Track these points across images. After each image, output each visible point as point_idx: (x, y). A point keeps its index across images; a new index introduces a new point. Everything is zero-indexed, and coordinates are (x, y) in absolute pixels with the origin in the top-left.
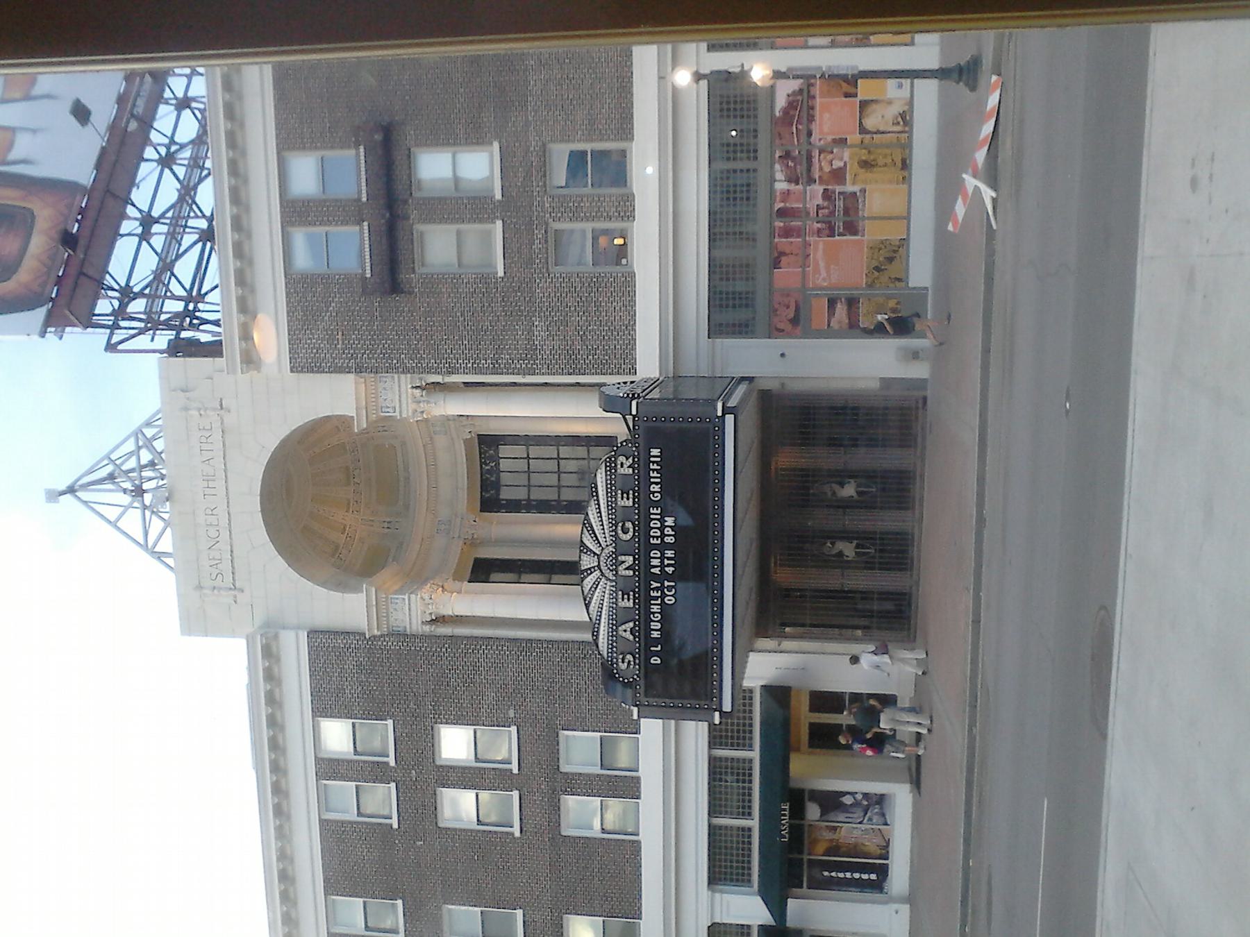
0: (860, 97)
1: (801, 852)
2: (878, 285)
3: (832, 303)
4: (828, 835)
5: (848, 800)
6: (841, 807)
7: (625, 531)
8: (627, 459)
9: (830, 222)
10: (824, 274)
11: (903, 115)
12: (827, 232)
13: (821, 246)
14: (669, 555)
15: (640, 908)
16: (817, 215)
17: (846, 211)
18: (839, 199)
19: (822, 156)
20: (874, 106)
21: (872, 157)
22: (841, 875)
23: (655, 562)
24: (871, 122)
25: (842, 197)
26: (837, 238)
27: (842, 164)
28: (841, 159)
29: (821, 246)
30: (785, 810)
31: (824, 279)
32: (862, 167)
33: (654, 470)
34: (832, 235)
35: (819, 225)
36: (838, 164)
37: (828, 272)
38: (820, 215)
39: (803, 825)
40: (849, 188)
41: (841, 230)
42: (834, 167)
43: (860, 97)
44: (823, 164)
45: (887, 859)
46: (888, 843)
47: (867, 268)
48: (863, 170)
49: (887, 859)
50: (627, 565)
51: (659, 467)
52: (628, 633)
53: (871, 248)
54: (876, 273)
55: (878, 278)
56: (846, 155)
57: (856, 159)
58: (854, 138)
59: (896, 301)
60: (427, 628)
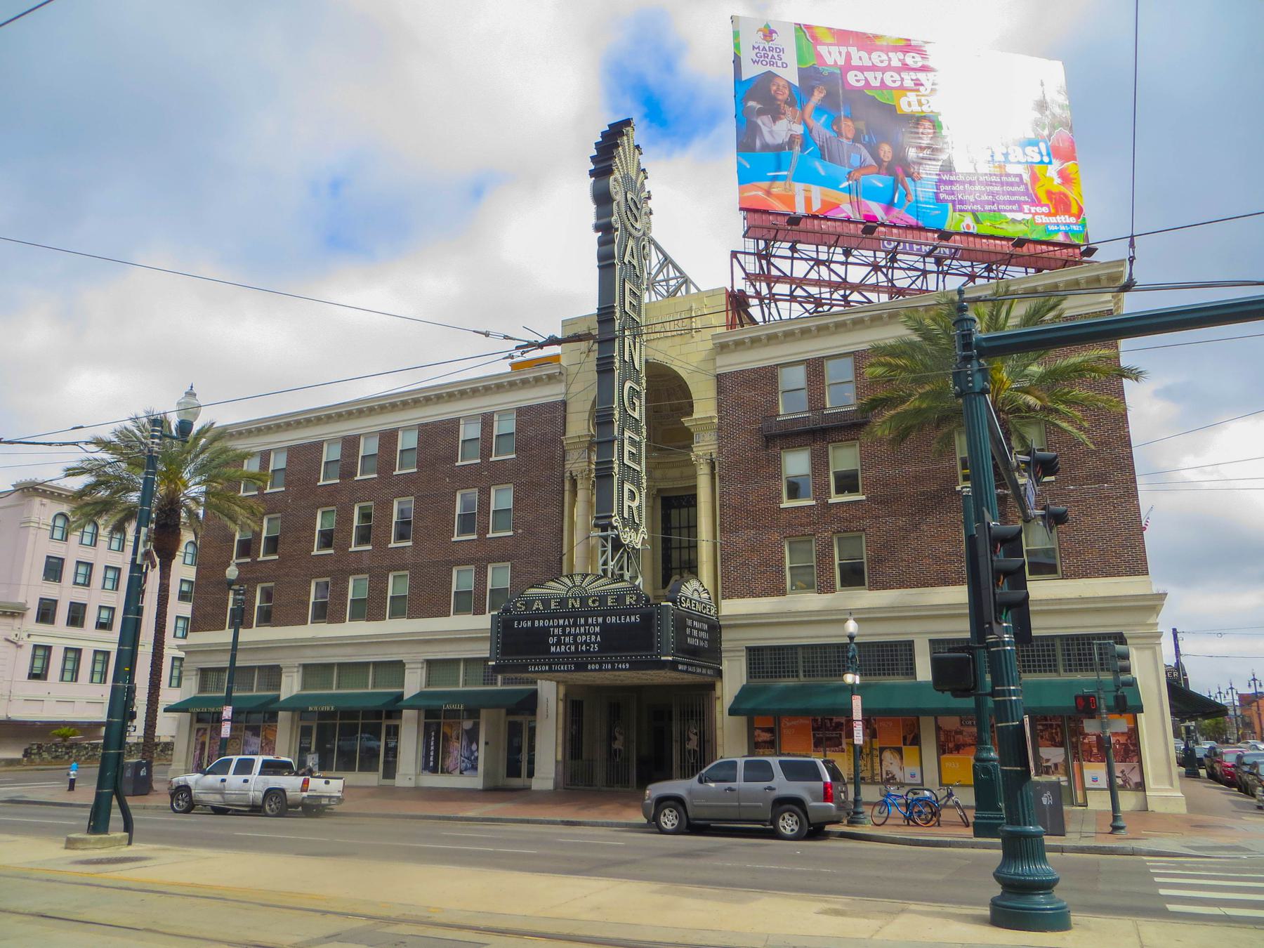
0: (904, 748)
3: (770, 730)
4: (454, 734)
5: (474, 747)
6: (470, 742)
7: (594, 602)
10: (788, 724)
11: (893, 778)
12: (815, 726)
17: (829, 739)
20: (898, 757)
21: (864, 756)
22: (432, 744)
23: (561, 622)
24: (887, 755)
29: (808, 722)
31: (785, 724)
35: (820, 720)
43: (904, 748)
45: (442, 772)
46: (449, 773)
49: (442, 772)
58: (877, 744)
60: (568, 474)
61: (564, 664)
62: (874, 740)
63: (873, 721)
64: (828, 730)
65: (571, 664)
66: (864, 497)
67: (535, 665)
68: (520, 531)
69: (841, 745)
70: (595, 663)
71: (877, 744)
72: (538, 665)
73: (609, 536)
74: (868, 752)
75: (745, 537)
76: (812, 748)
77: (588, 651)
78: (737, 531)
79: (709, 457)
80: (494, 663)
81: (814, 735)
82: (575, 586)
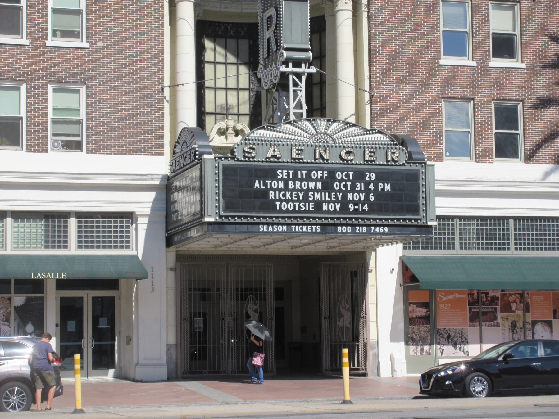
0: (554, 321)
2: (439, 338)
3: (426, 305)
8: (397, 157)
9: (478, 302)
12: (472, 300)
13: (464, 296)
14: (292, 184)
16: (482, 293)
17: (485, 313)
18: (492, 308)
19: (518, 295)
20: (548, 330)
21: (518, 330)
25: (494, 310)
26: (468, 307)
27: (514, 309)
28: (517, 309)
29: (464, 296)
30: (60, 275)
31: (441, 299)
32: (512, 323)
33: (322, 173)
34: (470, 304)
35: (476, 295)
36: (514, 306)
37: (448, 301)
38: (482, 295)
40: (499, 315)
41: (473, 310)
42: (512, 304)
43: (554, 321)
44: (513, 296)
47: (450, 330)
48: (510, 325)
50: (323, 154)
51: (324, 178)
52: (273, 153)
53: (462, 332)
54: (446, 336)
55: (443, 337)
56: (520, 312)
57: (517, 319)
58: (529, 318)
59: (428, 351)
61: (307, 225)
62: (527, 314)
63: (526, 295)
64: (484, 304)
65: (316, 225)
66: (523, 66)
67: (268, 224)
68: (100, 44)
69: (496, 318)
70: (347, 225)
72: (273, 224)
73: (303, 73)
74: (522, 326)
75: (400, 92)
76: (468, 323)
77: (356, 211)
80: (212, 220)
81: (470, 309)
82: (324, 134)
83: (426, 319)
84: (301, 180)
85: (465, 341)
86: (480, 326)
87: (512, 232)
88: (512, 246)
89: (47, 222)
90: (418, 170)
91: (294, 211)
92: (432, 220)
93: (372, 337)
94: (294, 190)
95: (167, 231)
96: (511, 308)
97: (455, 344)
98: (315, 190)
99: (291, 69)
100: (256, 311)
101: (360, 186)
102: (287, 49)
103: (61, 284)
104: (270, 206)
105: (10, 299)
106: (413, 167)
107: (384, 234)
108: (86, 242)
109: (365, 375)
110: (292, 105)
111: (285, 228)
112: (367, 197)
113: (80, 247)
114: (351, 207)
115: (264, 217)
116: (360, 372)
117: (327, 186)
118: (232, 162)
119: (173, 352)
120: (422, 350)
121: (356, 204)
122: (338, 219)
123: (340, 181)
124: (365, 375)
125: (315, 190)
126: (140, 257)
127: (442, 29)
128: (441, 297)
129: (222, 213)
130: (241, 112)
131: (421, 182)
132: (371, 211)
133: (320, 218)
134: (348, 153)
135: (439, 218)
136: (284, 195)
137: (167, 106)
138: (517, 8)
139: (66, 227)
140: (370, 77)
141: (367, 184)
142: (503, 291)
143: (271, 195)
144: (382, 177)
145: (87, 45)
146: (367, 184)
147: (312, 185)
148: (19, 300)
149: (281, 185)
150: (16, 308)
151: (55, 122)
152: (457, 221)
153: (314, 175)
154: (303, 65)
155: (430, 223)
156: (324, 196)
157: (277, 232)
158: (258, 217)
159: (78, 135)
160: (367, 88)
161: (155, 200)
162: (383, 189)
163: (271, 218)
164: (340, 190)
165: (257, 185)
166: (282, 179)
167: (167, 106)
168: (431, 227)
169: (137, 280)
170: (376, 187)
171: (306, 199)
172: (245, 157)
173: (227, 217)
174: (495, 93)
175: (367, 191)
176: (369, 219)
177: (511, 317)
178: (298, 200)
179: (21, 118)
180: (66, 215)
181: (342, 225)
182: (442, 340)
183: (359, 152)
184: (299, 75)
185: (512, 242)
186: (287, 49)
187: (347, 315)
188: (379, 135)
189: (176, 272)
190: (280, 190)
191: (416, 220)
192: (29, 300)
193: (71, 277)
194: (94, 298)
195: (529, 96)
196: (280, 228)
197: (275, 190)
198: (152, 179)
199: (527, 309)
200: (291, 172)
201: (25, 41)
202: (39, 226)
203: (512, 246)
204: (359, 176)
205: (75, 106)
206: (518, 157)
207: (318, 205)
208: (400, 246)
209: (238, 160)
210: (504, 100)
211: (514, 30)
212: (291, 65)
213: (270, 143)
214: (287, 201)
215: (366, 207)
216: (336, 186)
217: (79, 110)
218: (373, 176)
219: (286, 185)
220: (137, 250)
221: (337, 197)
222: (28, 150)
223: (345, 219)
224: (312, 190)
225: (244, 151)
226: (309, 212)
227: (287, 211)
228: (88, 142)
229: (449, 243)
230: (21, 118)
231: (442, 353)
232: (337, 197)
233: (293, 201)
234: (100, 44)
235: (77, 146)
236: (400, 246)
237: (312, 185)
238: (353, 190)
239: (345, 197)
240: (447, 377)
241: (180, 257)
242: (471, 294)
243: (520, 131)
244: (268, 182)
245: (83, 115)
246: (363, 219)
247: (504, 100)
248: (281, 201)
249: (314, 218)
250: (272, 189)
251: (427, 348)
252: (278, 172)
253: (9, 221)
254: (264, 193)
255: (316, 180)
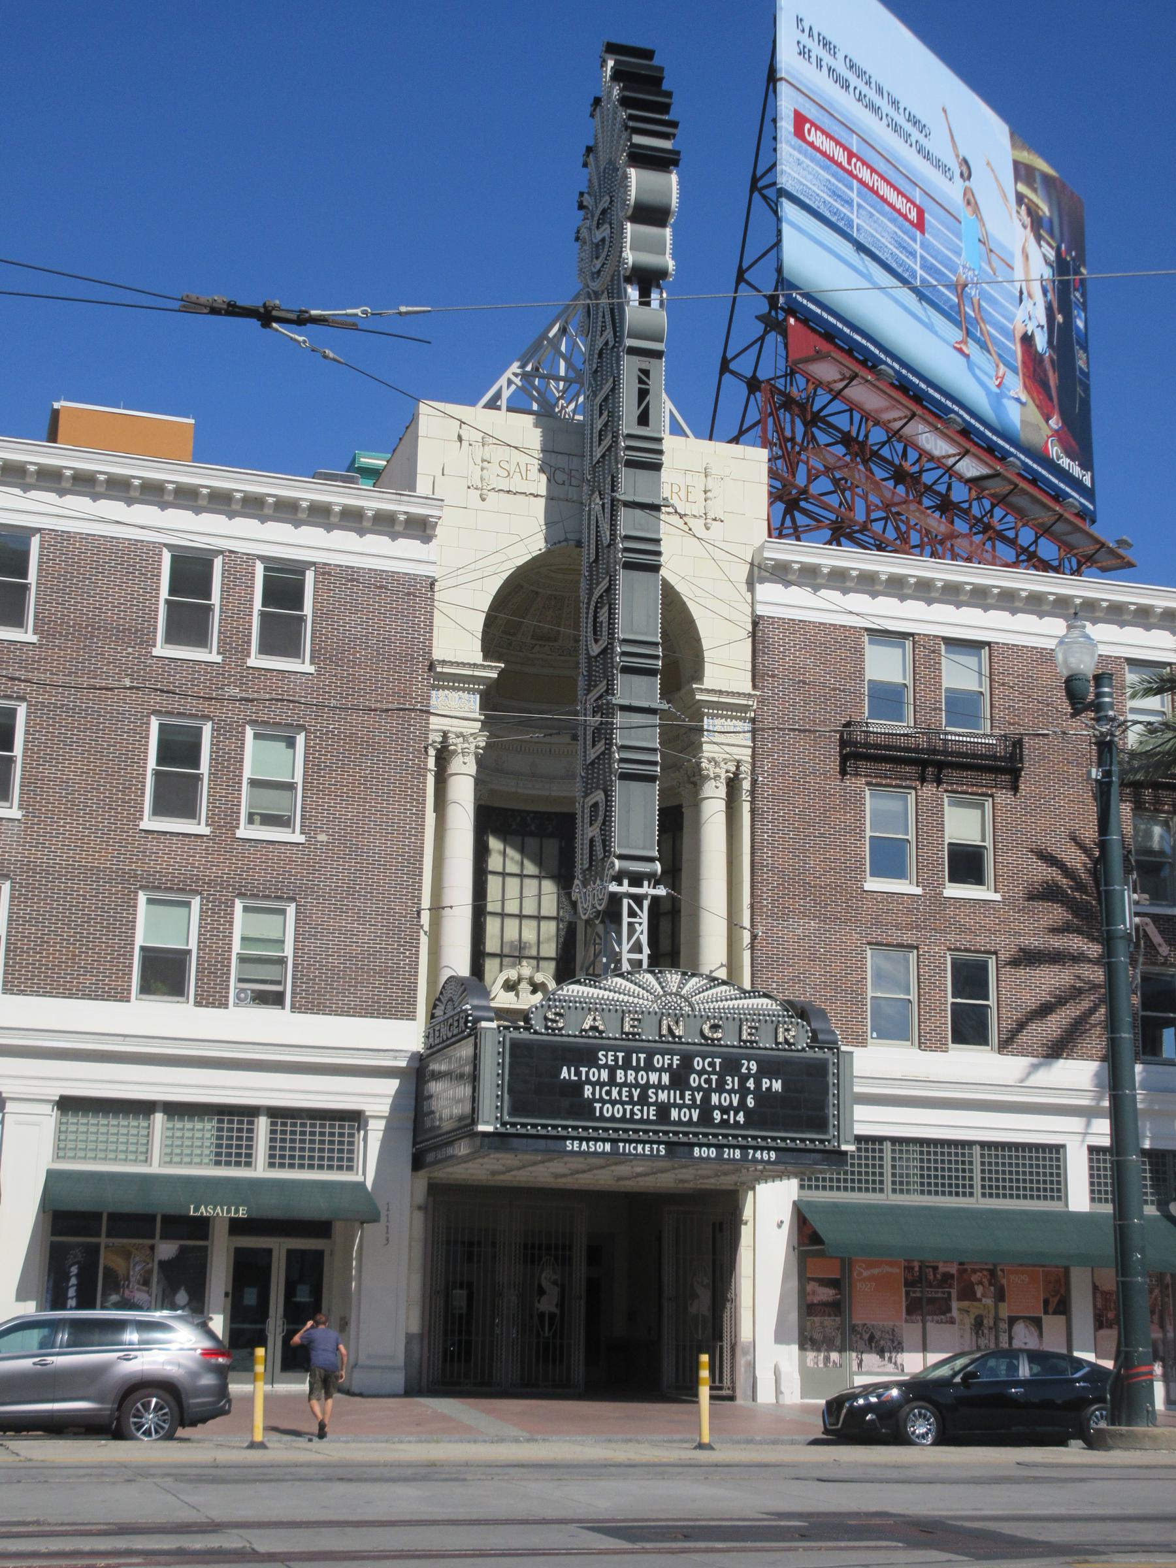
0: (1044, 1317)
1: (109, 1235)
2: (854, 1339)
3: (834, 1284)
4: (136, 1272)
7: (715, 1027)
8: (794, 1036)
9: (920, 1281)
10: (865, 1274)
13: (898, 1271)
15: (22, 992)
16: (928, 1267)
17: (931, 1301)
18: (943, 1293)
19: (986, 1273)
20: (1036, 1334)
25: (946, 1296)
26: (904, 1290)
27: (979, 1295)
28: (984, 1296)
29: (898, 1271)
30: (237, 1211)
31: (860, 1274)
32: (975, 1319)
33: (671, 1059)
34: (908, 1284)
35: (917, 1269)
36: (979, 1291)
38: (927, 1270)
39: (152, 1237)
40: (955, 1305)
41: (912, 1295)
42: (976, 1287)
43: (1044, 1317)
44: (979, 1274)
47: (873, 1326)
48: (973, 1322)
51: (675, 1067)
53: (893, 1330)
54: (866, 1337)
55: (861, 1338)
56: (989, 1301)
57: (984, 1313)
58: (1005, 1311)
59: (837, 1361)
61: (644, 1142)
62: (1001, 1305)
63: (1000, 1273)
64: (930, 1286)
65: (659, 1143)
66: (997, 897)
67: (581, 1139)
68: (322, 837)
69: (949, 1310)
70: (709, 1146)
71: (1004, 1313)
72: (588, 1140)
73: (645, 896)
74: (992, 1324)
75: (799, 931)
76: (904, 1315)
77: (724, 1123)
78: (784, 917)
79: (733, 769)
80: (490, 1129)
81: (907, 1293)
83: (835, 1308)
84: (637, 1069)
85: (899, 1348)
86: (924, 1322)
87: (977, 1167)
88: (978, 1190)
89: (220, 1121)
90: (827, 1060)
91: (623, 1119)
92: (847, 1142)
93: (745, 1334)
94: (625, 1084)
95: (415, 1143)
96: (974, 1293)
97: (881, 1352)
98: (659, 1086)
99: (625, 888)
100: (555, 1283)
101: (732, 1082)
102: (621, 857)
103: (237, 1227)
104: (584, 1110)
105: (152, 1248)
106: (819, 1054)
107: (769, 1162)
108: (282, 1157)
109: (732, 1398)
110: (626, 947)
111: (608, 1147)
112: (742, 1101)
113: (272, 1165)
114: (717, 1116)
115: (575, 1128)
116: (724, 1393)
117: (679, 1081)
118: (525, 1035)
119: (416, 1347)
120: (827, 1359)
121: (725, 1111)
122: (696, 1134)
123: (700, 1073)
124: (732, 1398)
125: (659, 1086)
126: (369, 1185)
127: (868, 833)
128: (861, 1272)
129: (506, 1118)
130: (543, 954)
131: (832, 1080)
132: (748, 1124)
133: (666, 1133)
134: (715, 1027)
135: (859, 1139)
136: (609, 1093)
137: (424, 941)
138: (988, 805)
139: (250, 1131)
140: (752, 907)
141: (744, 1079)
142: (961, 1264)
143: (588, 1091)
144: (768, 1068)
145: (301, 839)
146: (744, 1079)
147: (654, 1078)
148: (167, 1250)
149: (604, 1075)
150: (162, 1264)
151: (243, 959)
152: (887, 1146)
153: (658, 1061)
154: (646, 883)
155: (844, 1147)
156: (674, 1096)
157: (595, 1153)
158: (565, 1127)
159: (278, 983)
160: (746, 922)
161: (398, 1092)
162: (769, 1089)
163: (585, 1129)
164: (699, 1088)
165: (564, 1074)
166: (606, 1066)
167: (424, 941)
168: (845, 1153)
169: (362, 1223)
170: (758, 1084)
171: (643, 1100)
172: (547, 1028)
173: (513, 1125)
174: (953, 939)
175: (743, 1091)
176: (745, 1137)
177: (975, 1309)
178: (631, 1102)
179: (189, 952)
180: (252, 1112)
181: (701, 1145)
182: (861, 1344)
183: (732, 1027)
184: (638, 899)
185: (977, 1183)
186: (621, 857)
187: (705, 1296)
188: (765, 1001)
189: (426, 1214)
190: (602, 1085)
191: (822, 1141)
192: (183, 1250)
193: (254, 1215)
194: (290, 1253)
195: (1007, 946)
196: (600, 1147)
197: (593, 1084)
198: (395, 1058)
199: (1000, 1296)
200: (620, 1055)
201: (203, 829)
202: (206, 1128)
203: (978, 1190)
204: (731, 1065)
205: (275, 935)
206: (987, 1044)
207: (663, 1111)
208: (794, 1183)
209: (536, 1032)
210: (966, 950)
211: (983, 840)
212: (626, 882)
213: (589, 1007)
214: (613, 1103)
215: (741, 1118)
216: (694, 1081)
217: (283, 942)
218: (754, 1067)
219: (612, 1075)
220: (364, 1174)
221: (693, 1099)
222: (198, 1004)
223: (705, 1135)
224: (653, 1086)
225: (546, 1019)
226: (648, 1122)
227: (613, 1119)
228: (294, 993)
229: (964, 1186)
230: (189, 952)
231: (860, 1365)
232: (693, 1099)
233: (623, 1103)
234: (322, 837)
235: (276, 1000)
236: (794, 1183)
237: (654, 1078)
238: (721, 1088)
239: (706, 1099)
240: (869, 1408)
241: (435, 1189)
242: (909, 1269)
243: (992, 1002)
244: (584, 1070)
245: (289, 951)
246: (735, 1137)
247: (966, 950)
248: (603, 1102)
249: (656, 1132)
250: (588, 1081)
251: (834, 1356)
252: (600, 1054)
253: (159, 1118)
254: (578, 1087)
255: (661, 1070)
